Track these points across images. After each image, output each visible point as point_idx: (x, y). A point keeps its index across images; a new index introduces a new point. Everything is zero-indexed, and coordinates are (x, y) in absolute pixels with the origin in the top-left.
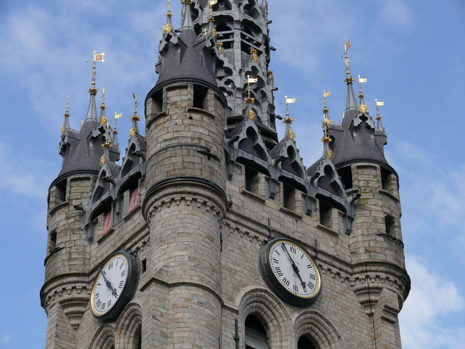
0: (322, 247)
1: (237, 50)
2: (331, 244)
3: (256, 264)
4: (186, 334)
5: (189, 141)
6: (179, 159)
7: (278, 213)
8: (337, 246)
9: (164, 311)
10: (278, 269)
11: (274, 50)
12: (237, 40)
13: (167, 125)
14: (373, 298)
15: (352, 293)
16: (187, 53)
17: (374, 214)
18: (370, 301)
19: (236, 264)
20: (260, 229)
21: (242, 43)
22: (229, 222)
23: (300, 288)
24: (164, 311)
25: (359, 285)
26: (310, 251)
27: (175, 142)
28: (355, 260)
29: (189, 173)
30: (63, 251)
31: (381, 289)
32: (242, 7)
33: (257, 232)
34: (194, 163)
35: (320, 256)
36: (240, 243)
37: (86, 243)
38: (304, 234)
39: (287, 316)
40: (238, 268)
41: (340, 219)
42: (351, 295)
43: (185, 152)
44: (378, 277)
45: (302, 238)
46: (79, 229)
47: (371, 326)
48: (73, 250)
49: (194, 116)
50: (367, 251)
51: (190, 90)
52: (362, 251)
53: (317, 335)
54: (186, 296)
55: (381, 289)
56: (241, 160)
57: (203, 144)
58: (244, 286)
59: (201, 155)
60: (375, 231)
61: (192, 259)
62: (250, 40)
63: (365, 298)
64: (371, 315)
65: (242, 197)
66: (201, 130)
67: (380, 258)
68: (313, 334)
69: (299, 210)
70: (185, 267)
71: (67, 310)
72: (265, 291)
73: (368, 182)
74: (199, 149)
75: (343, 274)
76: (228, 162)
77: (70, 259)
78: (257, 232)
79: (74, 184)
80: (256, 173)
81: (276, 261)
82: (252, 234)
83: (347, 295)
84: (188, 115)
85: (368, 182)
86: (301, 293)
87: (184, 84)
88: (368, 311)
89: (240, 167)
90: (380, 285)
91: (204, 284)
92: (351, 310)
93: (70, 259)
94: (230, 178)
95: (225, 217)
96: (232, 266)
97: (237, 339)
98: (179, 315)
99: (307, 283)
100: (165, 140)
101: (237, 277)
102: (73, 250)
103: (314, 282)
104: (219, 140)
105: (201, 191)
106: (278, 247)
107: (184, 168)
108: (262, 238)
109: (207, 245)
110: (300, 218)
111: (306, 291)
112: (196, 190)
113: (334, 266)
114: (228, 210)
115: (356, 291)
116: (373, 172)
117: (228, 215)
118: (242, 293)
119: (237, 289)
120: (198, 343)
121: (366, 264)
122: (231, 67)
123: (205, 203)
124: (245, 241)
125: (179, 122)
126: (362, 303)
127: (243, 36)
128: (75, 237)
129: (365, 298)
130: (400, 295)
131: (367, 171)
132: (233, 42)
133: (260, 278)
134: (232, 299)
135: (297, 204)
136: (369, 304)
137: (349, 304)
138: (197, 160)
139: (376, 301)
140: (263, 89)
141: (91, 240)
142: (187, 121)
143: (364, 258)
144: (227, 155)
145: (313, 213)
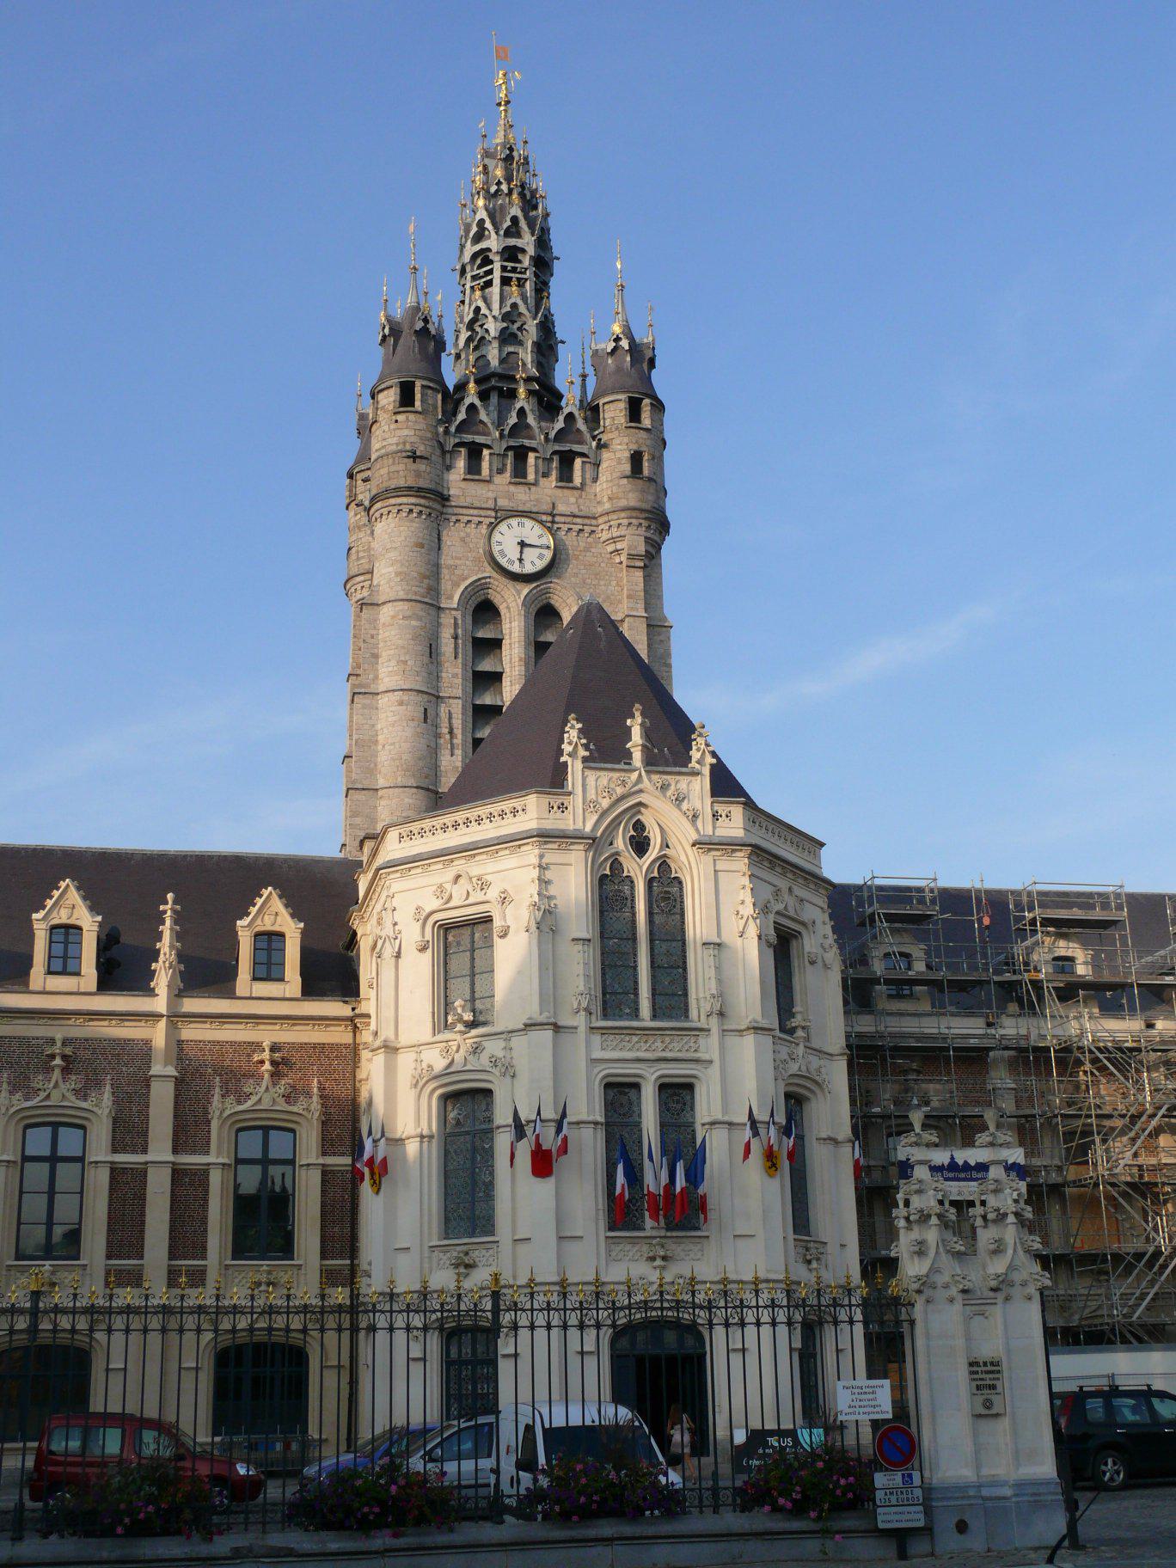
0: (561, 508)
1: (495, 289)
3: (481, 551)
5: (394, 448)
8: (581, 501)
10: (502, 552)
11: (558, 259)
12: (497, 275)
16: (401, 341)
17: (618, 455)
19: (457, 558)
20: (483, 513)
22: (447, 516)
26: (544, 518)
27: (383, 451)
30: (353, 551)
34: (398, 472)
36: (462, 534)
38: (537, 500)
45: (535, 506)
48: (360, 548)
49: (400, 418)
52: (605, 499)
57: (408, 447)
58: (466, 579)
59: (406, 460)
60: (619, 474)
62: (514, 270)
66: (406, 432)
70: (392, 584)
74: (404, 454)
81: (500, 543)
82: (476, 519)
83: (593, 550)
90: (623, 533)
92: (597, 565)
93: (358, 559)
102: (360, 548)
106: (503, 527)
118: (462, 588)
125: (386, 428)
127: (504, 269)
128: (361, 535)
132: (492, 280)
138: (401, 467)
142: (393, 426)
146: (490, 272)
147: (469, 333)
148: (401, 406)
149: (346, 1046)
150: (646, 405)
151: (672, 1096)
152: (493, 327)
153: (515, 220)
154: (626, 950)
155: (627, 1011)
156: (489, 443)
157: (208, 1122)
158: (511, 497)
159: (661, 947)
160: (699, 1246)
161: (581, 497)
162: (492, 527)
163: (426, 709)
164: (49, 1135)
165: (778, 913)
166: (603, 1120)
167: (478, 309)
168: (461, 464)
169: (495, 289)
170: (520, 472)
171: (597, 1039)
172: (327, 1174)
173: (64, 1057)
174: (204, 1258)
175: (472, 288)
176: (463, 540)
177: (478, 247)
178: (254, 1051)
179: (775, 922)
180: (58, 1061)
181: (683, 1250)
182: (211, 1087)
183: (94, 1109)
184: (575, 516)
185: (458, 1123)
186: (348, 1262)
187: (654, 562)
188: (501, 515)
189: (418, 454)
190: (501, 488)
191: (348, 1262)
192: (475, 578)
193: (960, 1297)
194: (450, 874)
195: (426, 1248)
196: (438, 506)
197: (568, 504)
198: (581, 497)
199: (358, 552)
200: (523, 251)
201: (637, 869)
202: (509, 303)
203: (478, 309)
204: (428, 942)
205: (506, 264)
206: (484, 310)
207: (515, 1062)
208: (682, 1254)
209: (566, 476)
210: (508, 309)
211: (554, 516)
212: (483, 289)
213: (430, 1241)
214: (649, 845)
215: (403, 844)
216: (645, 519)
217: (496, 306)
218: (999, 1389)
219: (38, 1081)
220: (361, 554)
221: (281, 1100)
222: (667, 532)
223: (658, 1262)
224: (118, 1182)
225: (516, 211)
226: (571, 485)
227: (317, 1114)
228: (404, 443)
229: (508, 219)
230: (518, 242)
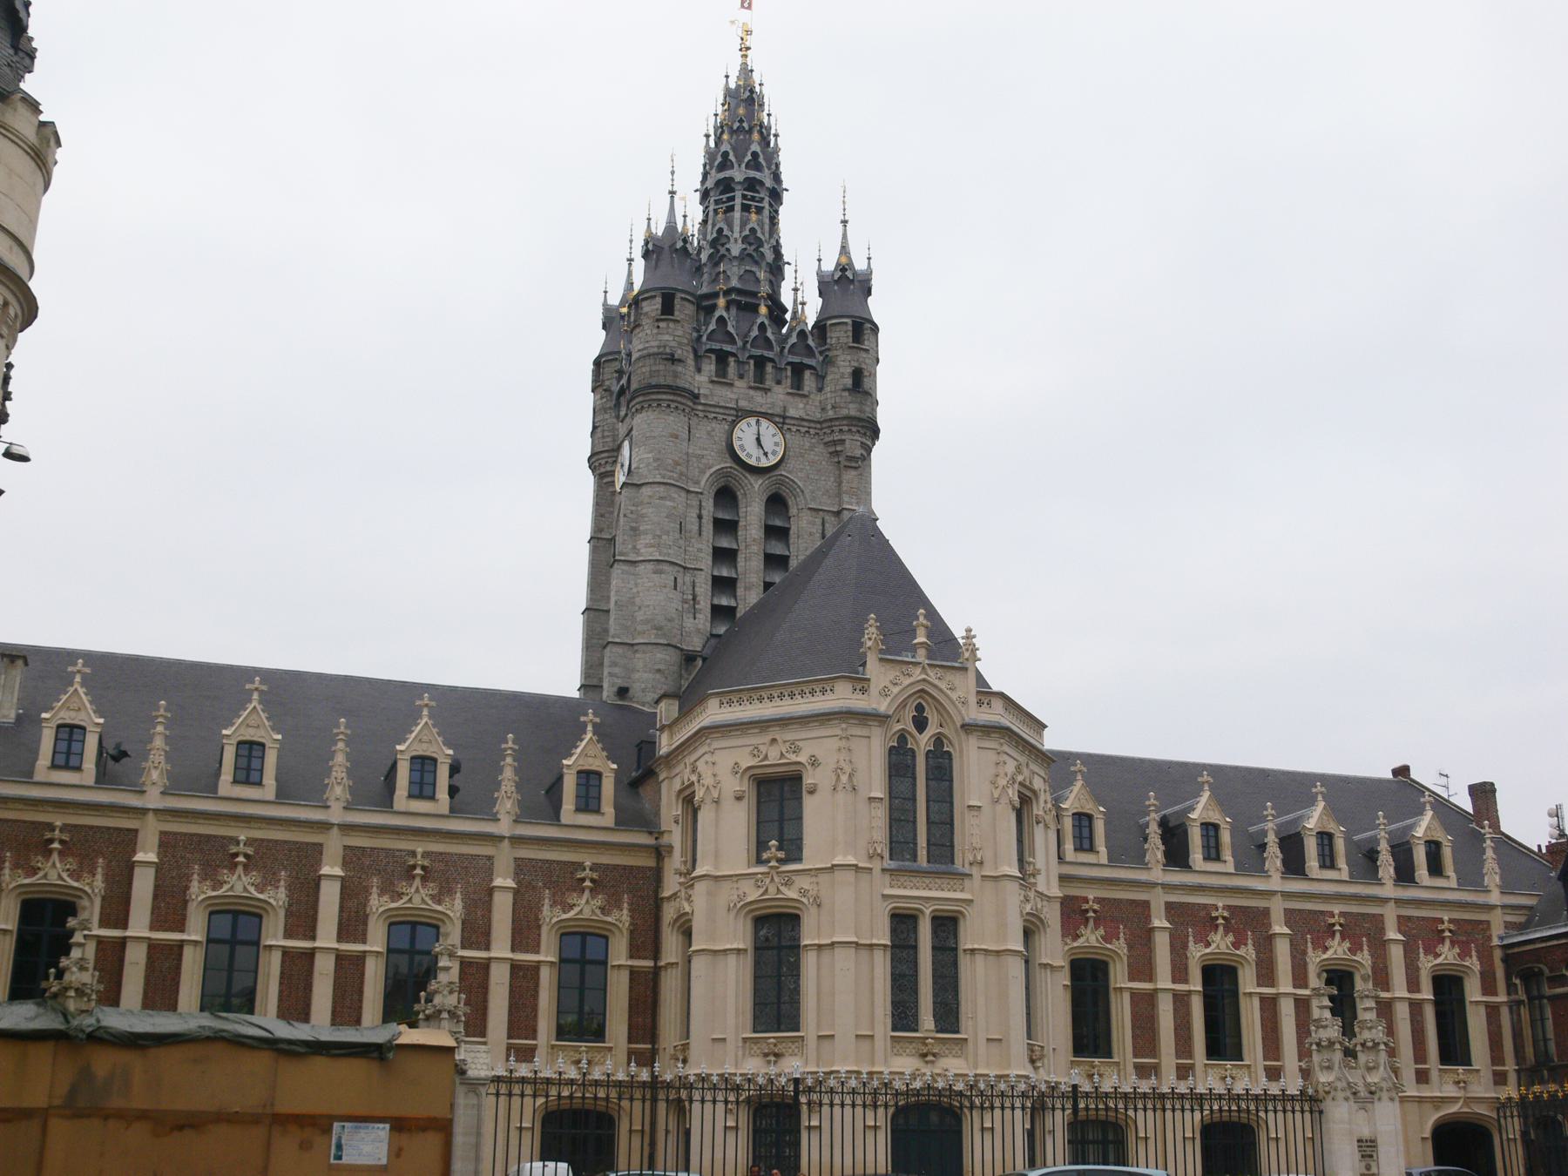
0: (792, 412)
1: (737, 214)
2: (801, 406)
4: (648, 527)
5: (656, 350)
6: (648, 369)
7: (747, 391)
8: (808, 407)
9: (634, 508)
10: (742, 447)
11: (787, 190)
12: (738, 202)
13: (640, 335)
14: (839, 448)
15: (822, 446)
18: (836, 451)
21: (742, 204)
23: (763, 458)
24: (634, 508)
25: (827, 439)
26: (777, 419)
27: (645, 352)
28: (825, 416)
29: (654, 381)
30: (599, 429)
31: (844, 440)
32: (743, 165)
33: (725, 414)
35: (787, 421)
36: (709, 428)
37: (615, 420)
38: (773, 404)
39: (751, 484)
40: (705, 452)
41: (813, 378)
42: (820, 449)
43: (652, 361)
44: (841, 430)
46: (610, 408)
47: (837, 472)
48: (606, 428)
49: (662, 325)
50: (833, 407)
51: (659, 300)
52: (829, 407)
53: (785, 492)
54: (650, 494)
55: (844, 440)
56: (711, 351)
57: (668, 350)
58: (710, 468)
60: (842, 387)
61: (656, 460)
62: (753, 199)
63: (832, 449)
64: (839, 462)
65: (710, 386)
67: (844, 412)
68: (781, 492)
69: (769, 383)
71: (605, 480)
72: (731, 467)
73: (838, 338)
74: (664, 356)
75: (812, 431)
76: (697, 358)
77: (603, 437)
78: (725, 414)
79: (606, 365)
80: (727, 357)
81: (740, 439)
82: (720, 417)
84: (656, 324)
85: (838, 338)
86: (764, 463)
87: (653, 294)
88: (836, 460)
89: (710, 357)
91: (665, 481)
94: (699, 370)
95: (693, 409)
96: (699, 452)
97: (700, 517)
98: (644, 511)
99: (770, 452)
100: (639, 351)
101: (704, 461)
103: (777, 449)
104: (686, 341)
105: (664, 397)
106: (743, 424)
107: (651, 377)
108: (730, 419)
109: (671, 444)
110: (769, 390)
111: (768, 459)
112: (660, 397)
113: (803, 426)
114: (694, 403)
115: (826, 443)
116: (844, 328)
117: (696, 407)
118: (708, 475)
119: (702, 472)
120: (658, 533)
121: (831, 420)
122: (729, 234)
123: (669, 406)
124: (714, 425)
125: (649, 332)
126: (831, 453)
127: (744, 197)
128: (607, 416)
129: (832, 449)
130: (864, 440)
131: (838, 328)
133: (727, 456)
134: (697, 483)
135: (767, 376)
136: (837, 453)
137: (817, 458)
138: (662, 367)
139: (842, 451)
140: (762, 249)
141: (617, 417)
142: (655, 331)
143: (831, 414)
144: (695, 352)
145: (784, 381)
146: (733, 199)
147: (712, 251)
148: (662, 314)
149: (650, 869)
152: (736, 249)
153: (755, 155)
155: (908, 857)
156: (734, 351)
157: (539, 927)
158: (750, 399)
159: (935, 807)
161: (807, 404)
162: (734, 424)
163: (676, 578)
164: (588, 951)
165: (1020, 783)
167: (720, 231)
168: (710, 367)
169: (737, 214)
170: (760, 377)
171: (887, 878)
172: (634, 974)
173: (424, 868)
174: (535, 1038)
175: (716, 211)
176: (709, 433)
177: (721, 175)
178: (576, 870)
179: (1019, 792)
180: (418, 871)
182: (541, 899)
183: (448, 912)
184: (803, 420)
185: (767, 939)
186: (649, 1046)
187: (865, 463)
188: (741, 414)
189: (676, 356)
190: (739, 392)
191: (649, 1046)
192: (719, 467)
193: (1351, 1097)
194: (767, 738)
196: (691, 404)
197: (797, 409)
198: (807, 404)
199: (603, 431)
200: (762, 183)
201: (922, 742)
202: (748, 227)
203: (720, 231)
205: (746, 193)
206: (726, 232)
208: (947, 1052)
209: (798, 384)
210: (747, 232)
211: (784, 417)
214: (927, 724)
215: (723, 710)
216: (862, 427)
217: (737, 228)
218: (1375, 1158)
219: (402, 886)
220: (606, 434)
221: (598, 912)
222: (878, 438)
223: (930, 1058)
224: (466, 974)
225: (755, 147)
226: (801, 392)
227: (627, 924)
228: (665, 347)
229: (749, 154)
230: (757, 175)
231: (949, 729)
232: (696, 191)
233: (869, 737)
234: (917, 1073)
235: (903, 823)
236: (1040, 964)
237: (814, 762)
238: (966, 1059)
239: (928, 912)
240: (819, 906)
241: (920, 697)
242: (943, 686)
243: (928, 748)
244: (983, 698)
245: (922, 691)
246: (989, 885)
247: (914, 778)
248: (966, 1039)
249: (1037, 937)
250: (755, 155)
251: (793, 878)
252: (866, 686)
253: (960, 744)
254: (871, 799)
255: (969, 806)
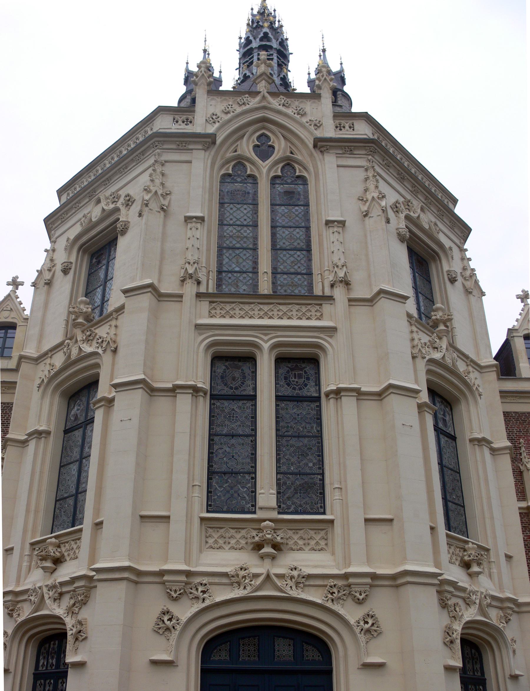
11: (292, 54)
132: (253, 61)
146: (253, 57)
150: (339, 94)
151: (292, 369)
154: (245, 234)
160: (322, 533)
166: (207, 387)
167: (245, 74)
171: (205, 305)
177: (246, 49)
181: (301, 538)
195: (28, 546)
204: (71, 263)
207: (118, 340)
208: (301, 542)
212: (248, 66)
213: (33, 537)
223: (267, 549)
231: (302, 154)
232: (236, 69)
233: (190, 162)
234: (242, 573)
235: (237, 252)
236: (471, 440)
237: (129, 202)
238: (333, 554)
239: (266, 346)
240: (115, 351)
241: (264, 128)
242: (289, 111)
243: (272, 174)
244: (343, 122)
245: (264, 120)
246: (361, 311)
247: (255, 204)
248: (332, 522)
249: (463, 406)
250: (266, 34)
251: (97, 331)
252: (190, 117)
253: (315, 167)
254: (188, 219)
255: (328, 223)
